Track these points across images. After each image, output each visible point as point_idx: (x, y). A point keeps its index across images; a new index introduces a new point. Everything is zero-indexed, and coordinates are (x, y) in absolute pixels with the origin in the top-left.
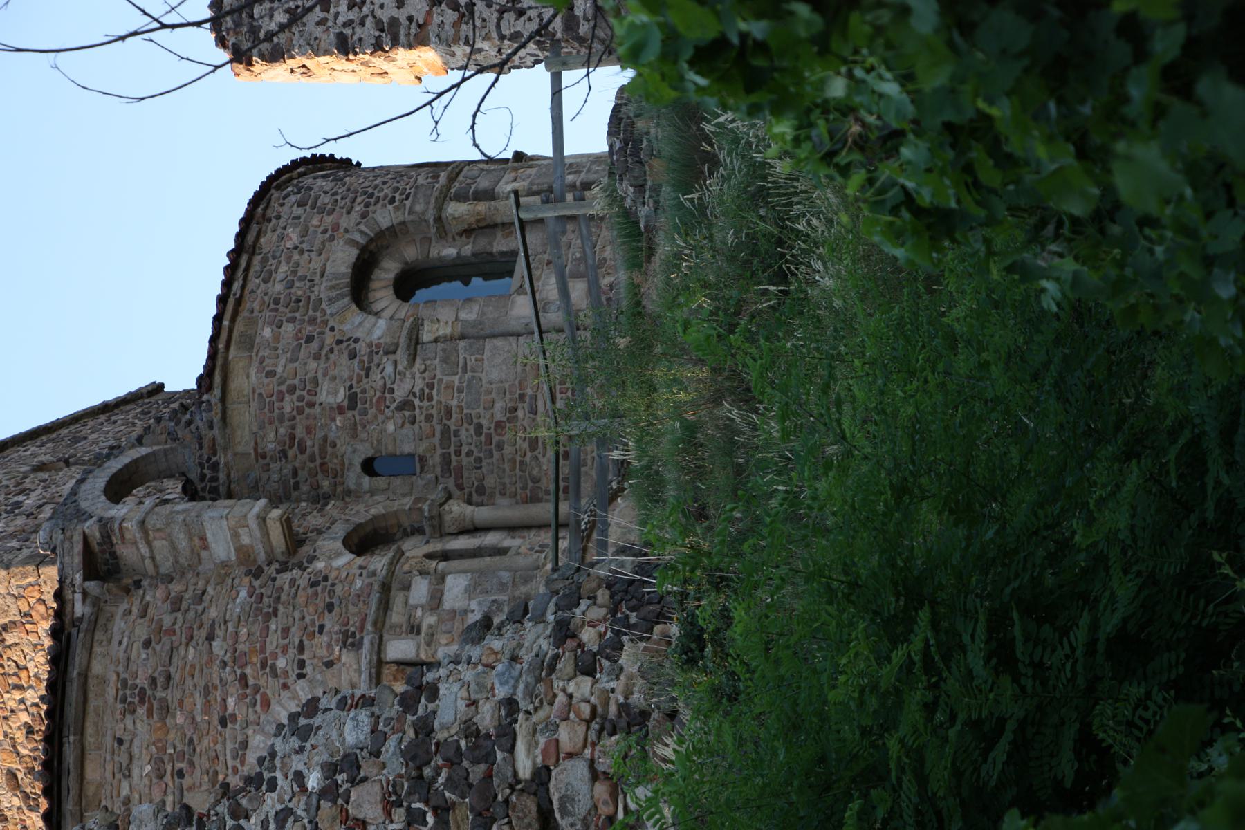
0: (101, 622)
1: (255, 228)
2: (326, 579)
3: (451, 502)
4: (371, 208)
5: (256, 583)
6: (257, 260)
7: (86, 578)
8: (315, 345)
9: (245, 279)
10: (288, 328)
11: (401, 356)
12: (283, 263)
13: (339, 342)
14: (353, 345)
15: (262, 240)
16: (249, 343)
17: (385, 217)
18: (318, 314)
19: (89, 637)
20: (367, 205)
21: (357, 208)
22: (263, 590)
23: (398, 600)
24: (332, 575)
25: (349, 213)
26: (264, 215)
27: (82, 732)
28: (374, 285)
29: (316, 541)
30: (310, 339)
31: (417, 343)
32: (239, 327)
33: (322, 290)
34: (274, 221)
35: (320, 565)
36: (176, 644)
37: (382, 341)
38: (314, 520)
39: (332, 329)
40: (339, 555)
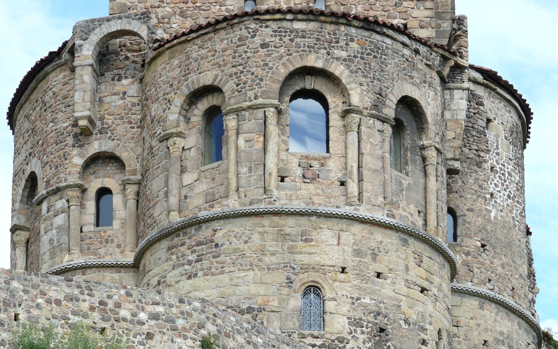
0: (63, 67)
1: (224, 24)
2: (66, 159)
3: (136, 186)
4: (234, 77)
5: (70, 128)
6: (212, 35)
7: (68, 52)
8: (169, 89)
9: (197, 37)
10: (177, 71)
11: (163, 134)
12: (207, 50)
13: (169, 101)
14: (167, 108)
15: (222, 31)
16: (172, 57)
17: (228, 88)
18: (183, 82)
19: (56, 67)
20: (236, 74)
21: (234, 70)
22: (65, 133)
23: (57, 197)
24: (67, 161)
25: (233, 66)
26: (233, 24)
27: (38, 83)
28: (210, 97)
29: (100, 139)
30: (171, 86)
31: (167, 139)
32: (179, 48)
33: (193, 77)
34: (232, 31)
35: (75, 151)
36: (52, 107)
37: (168, 122)
38: (121, 129)
39: (176, 93)
40: (82, 157)
